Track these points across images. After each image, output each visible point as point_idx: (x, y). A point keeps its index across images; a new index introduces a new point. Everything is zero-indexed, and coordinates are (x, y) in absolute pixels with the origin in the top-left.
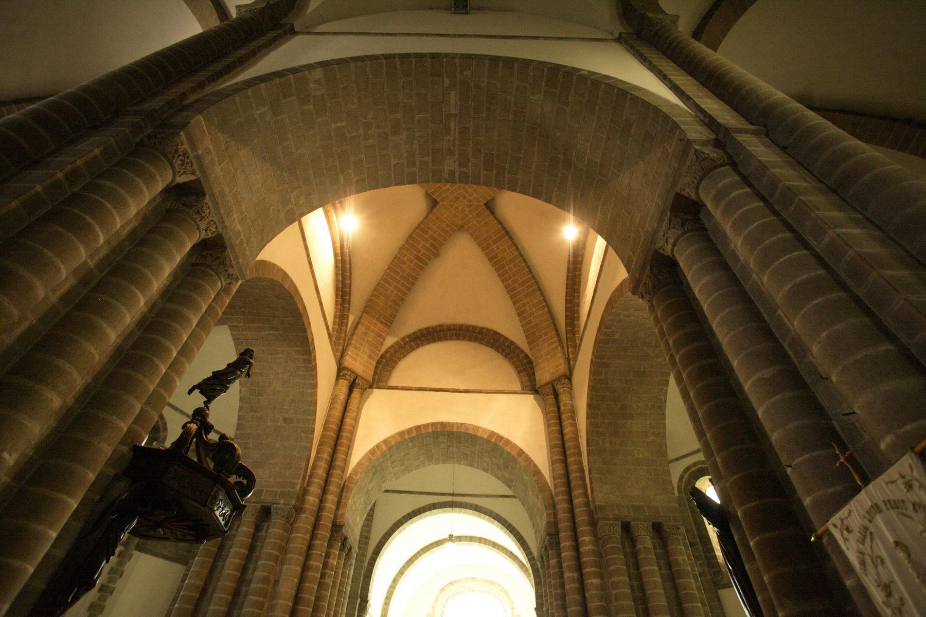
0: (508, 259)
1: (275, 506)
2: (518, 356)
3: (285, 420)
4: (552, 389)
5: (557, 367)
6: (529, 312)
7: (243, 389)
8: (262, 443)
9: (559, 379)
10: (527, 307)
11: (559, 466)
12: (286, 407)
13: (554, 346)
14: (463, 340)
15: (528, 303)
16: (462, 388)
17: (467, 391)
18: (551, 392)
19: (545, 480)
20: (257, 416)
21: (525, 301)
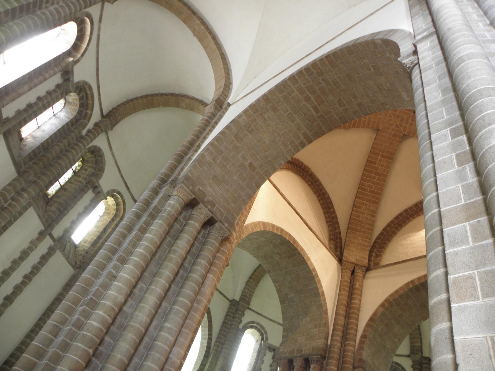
0: (379, 172)
1: (221, 224)
2: (335, 229)
3: (251, 164)
4: (353, 268)
5: (362, 258)
6: (363, 211)
7: (243, 117)
8: (226, 166)
9: (361, 267)
10: (364, 207)
11: (342, 321)
12: (258, 157)
13: (366, 244)
14: (312, 188)
15: (366, 205)
16: (309, 224)
17: (310, 229)
18: (352, 269)
19: (328, 321)
20: (235, 144)
21: (365, 202)
